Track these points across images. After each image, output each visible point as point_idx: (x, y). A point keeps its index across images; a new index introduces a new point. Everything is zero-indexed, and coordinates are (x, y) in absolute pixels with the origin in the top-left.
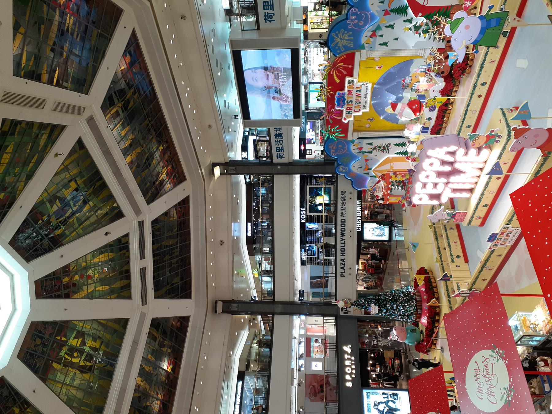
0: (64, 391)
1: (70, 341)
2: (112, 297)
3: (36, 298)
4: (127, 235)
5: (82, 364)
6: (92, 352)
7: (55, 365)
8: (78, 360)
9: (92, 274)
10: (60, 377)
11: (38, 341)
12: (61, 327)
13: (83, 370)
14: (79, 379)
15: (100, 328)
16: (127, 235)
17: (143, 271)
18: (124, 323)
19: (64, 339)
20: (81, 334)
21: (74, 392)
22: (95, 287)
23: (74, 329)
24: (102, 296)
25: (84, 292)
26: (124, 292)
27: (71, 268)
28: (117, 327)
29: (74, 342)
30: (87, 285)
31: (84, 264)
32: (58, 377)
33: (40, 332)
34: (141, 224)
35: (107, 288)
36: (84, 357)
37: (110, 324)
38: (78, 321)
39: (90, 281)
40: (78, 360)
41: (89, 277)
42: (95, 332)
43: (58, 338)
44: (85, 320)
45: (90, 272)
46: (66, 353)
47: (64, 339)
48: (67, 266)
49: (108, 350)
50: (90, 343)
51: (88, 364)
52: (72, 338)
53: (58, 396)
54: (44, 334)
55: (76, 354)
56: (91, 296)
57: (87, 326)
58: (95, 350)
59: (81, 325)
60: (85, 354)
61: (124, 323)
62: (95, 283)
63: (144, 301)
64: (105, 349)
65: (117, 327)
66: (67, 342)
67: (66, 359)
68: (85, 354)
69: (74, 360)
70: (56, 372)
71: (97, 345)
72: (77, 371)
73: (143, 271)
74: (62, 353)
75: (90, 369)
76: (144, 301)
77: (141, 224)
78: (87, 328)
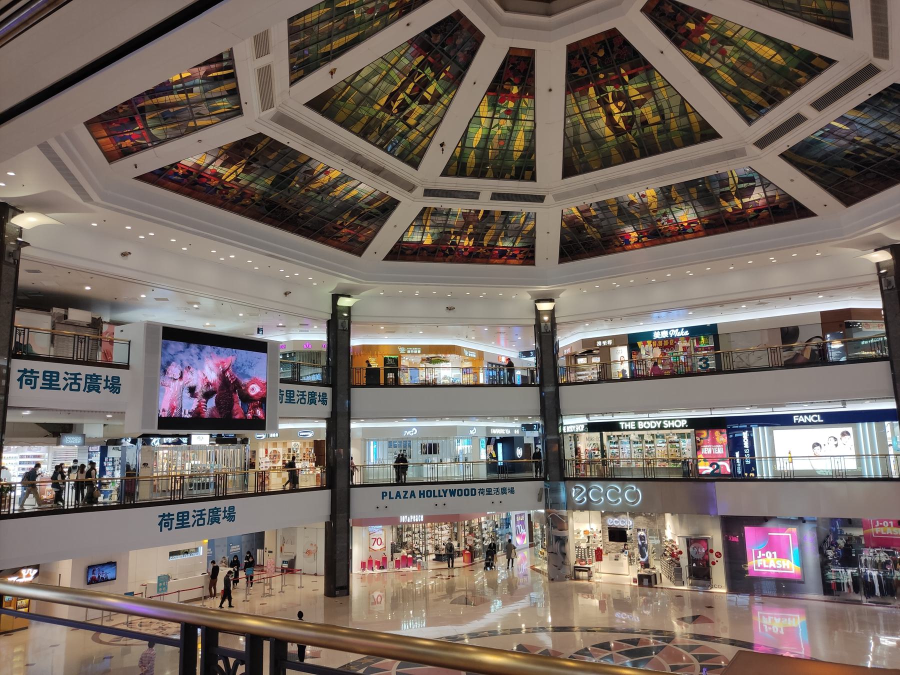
0: (575, 119)
1: (630, 87)
2: (730, 98)
3: (642, 10)
4: (830, 62)
5: (617, 118)
6: (638, 120)
7: (592, 91)
8: (616, 110)
9: (729, 52)
10: (585, 104)
11: (601, 53)
12: (638, 64)
13: (611, 123)
14: (601, 125)
15: (677, 110)
16: (830, 62)
17: (798, 120)
18: (708, 133)
19: (626, 78)
20: (650, 91)
21: (583, 128)
22: (719, 68)
23: (650, 79)
24: (719, 86)
25: (702, 59)
26: (749, 111)
27: (709, 22)
28: (696, 128)
29: (633, 91)
30: (712, 56)
31: (729, 34)
32: (583, 102)
33: (612, 46)
34: (870, 71)
35: (733, 83)
36: (626, 114)
37: (693, 117)
38: (663, 77)
39: (719, 56)
40: (616, 110)
41: (723, 53)
42: (665, 105)
43: (623, 71)
44: (669, 85)
45: (729, 49)
46: (613, 92)
47: (626, 78)
48: (706, 14)
49: (656, 136)
50: (647, 111)
51: (622, 125)
52: (635, 86)
53: (565, 117)
54: (613, 52)
55: (621, 104)
56: (704, 70)
57: (664, 93)
58: (645, 123)
59: (661, 84)
60: (630, 114)
61: (708, 133)
62: (724, 63)
63: (762, 143)
64: (655, 132)
65: (696, 128)
66: (627, 84)
67: (607, 97)
68: (630, 114)
69: (613, 107)
70: (585, 97)
71: (652, 119)
72: (604, 119)
73: (798, 120)
74: (610, 88)
75: (617, 132)
76: (762, 143)
77: (870, 71)
78: (663, 94)
